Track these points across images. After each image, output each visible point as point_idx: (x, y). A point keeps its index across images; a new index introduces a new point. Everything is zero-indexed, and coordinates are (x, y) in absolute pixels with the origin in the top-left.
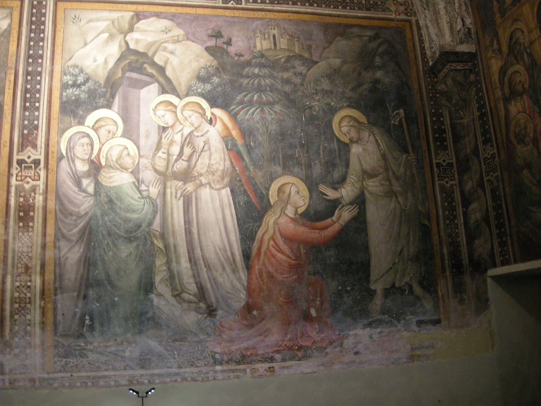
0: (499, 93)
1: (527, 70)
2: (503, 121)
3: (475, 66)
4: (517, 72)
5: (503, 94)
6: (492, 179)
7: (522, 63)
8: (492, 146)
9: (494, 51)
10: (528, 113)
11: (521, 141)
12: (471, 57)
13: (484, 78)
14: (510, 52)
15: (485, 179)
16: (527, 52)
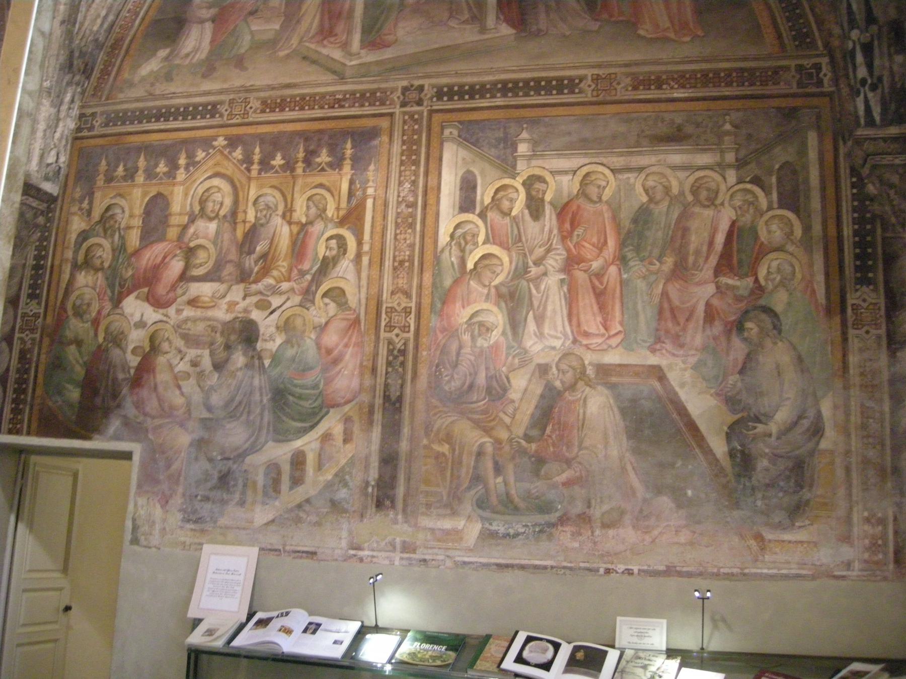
0: (69, 254)
1: (113, 250)
2: (63, 286)
3: (49, 210)
4: (100, 245)
5: (75, 259)
6: (26, 339)
7: (110, 240)
8: (39, 304)
9: (81, 209)
10: (98, 290)
11: (79, 313)
12: (51, 200)
13: (57, 230)
14: (100, 221)
15: (17, 335)
16: (120, 233)
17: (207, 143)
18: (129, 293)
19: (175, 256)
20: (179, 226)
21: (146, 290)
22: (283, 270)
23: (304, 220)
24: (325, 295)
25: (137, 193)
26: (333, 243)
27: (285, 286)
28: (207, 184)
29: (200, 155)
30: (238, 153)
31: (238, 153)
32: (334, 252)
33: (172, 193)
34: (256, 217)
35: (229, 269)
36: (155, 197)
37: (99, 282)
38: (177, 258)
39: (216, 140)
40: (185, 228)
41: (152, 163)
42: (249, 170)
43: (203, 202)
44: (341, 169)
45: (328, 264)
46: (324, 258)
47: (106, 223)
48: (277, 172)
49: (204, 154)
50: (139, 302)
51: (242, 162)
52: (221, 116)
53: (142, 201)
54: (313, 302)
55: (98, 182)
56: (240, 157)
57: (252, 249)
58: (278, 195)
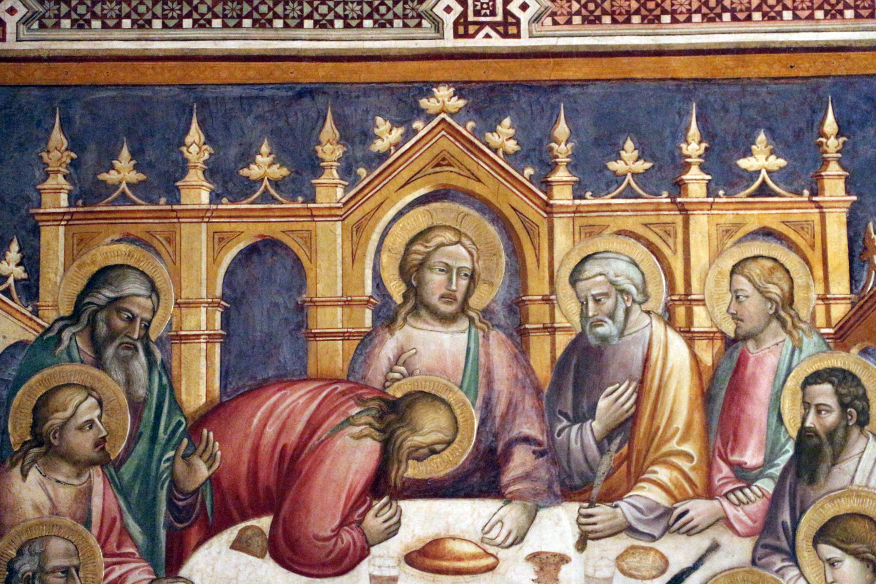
1: (137, 407)
7: (120, 377)
14: (74, 318)
16: (149, 353)
17: (406, 102)
18: (210, 532)
19: (349, 421)
20: (345, 336)
21: (265, 522)
22: (686, 466)
23: (729, 328)
24: (823, 535)
25: (196, 239)
26: (824, 393)
27: (700, 509)
28: (418, 220)
29: (386, 135)
30: (504, 136)
31: (504, 136)
32: (831, 419)
33: (309, 240)
34: (584, 315)
35: (521, 460)
36: (251, 251)
37: (97, 502)
38: (356, 430)
39: (429, 94)
40: (366, 342)
41: (233, 151)
42: (546, 186)
43: (412, 272)
44: (814, 193)
45: (817, 451)
46: (804, 434)
47: (98, 318)
48: (629, 193)
49: (397, 133)
50: (244, 557)
51: (518, 159)
52: (438, 24)
53: (214, 261)
54: (792, 556)
55: (46, 198)
56: (512, 146)
57: (585, 405)
58: (640, 252)
